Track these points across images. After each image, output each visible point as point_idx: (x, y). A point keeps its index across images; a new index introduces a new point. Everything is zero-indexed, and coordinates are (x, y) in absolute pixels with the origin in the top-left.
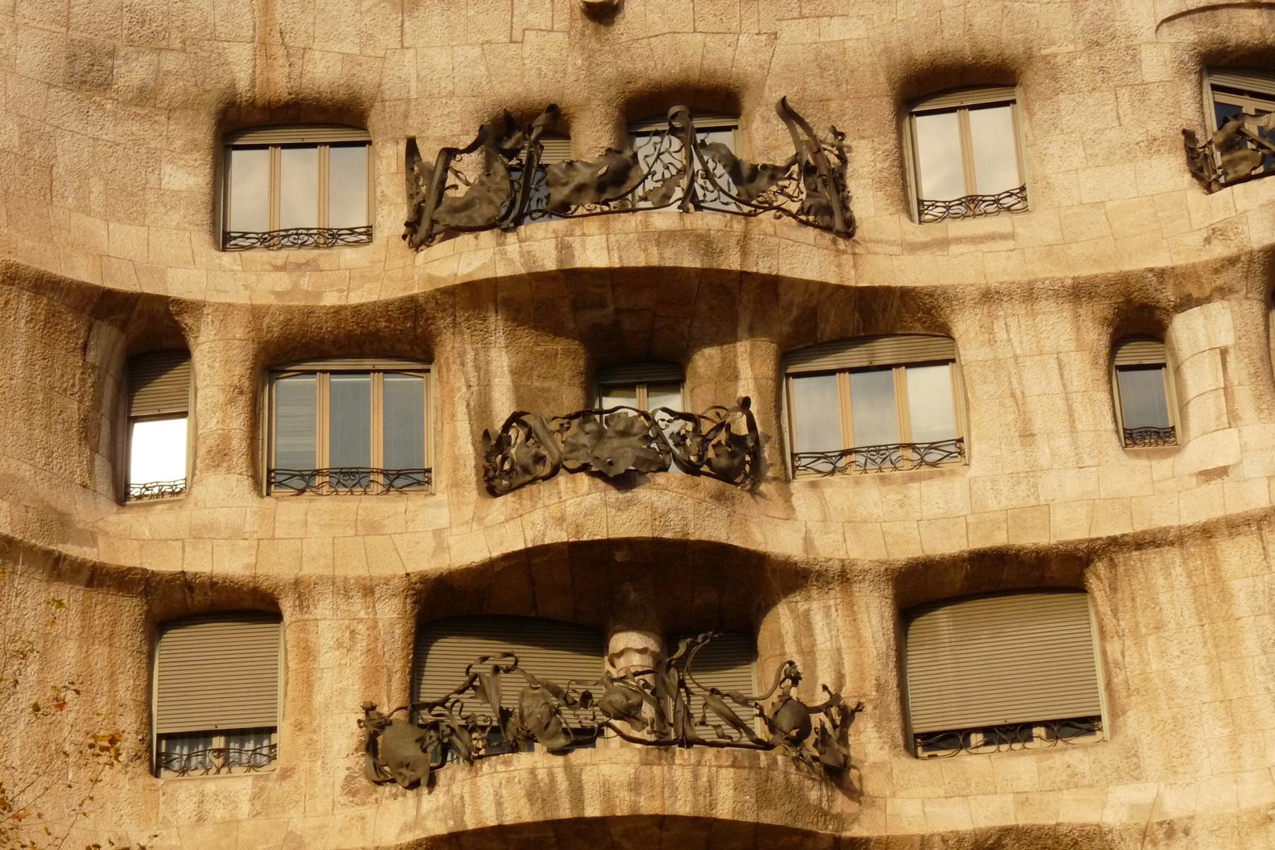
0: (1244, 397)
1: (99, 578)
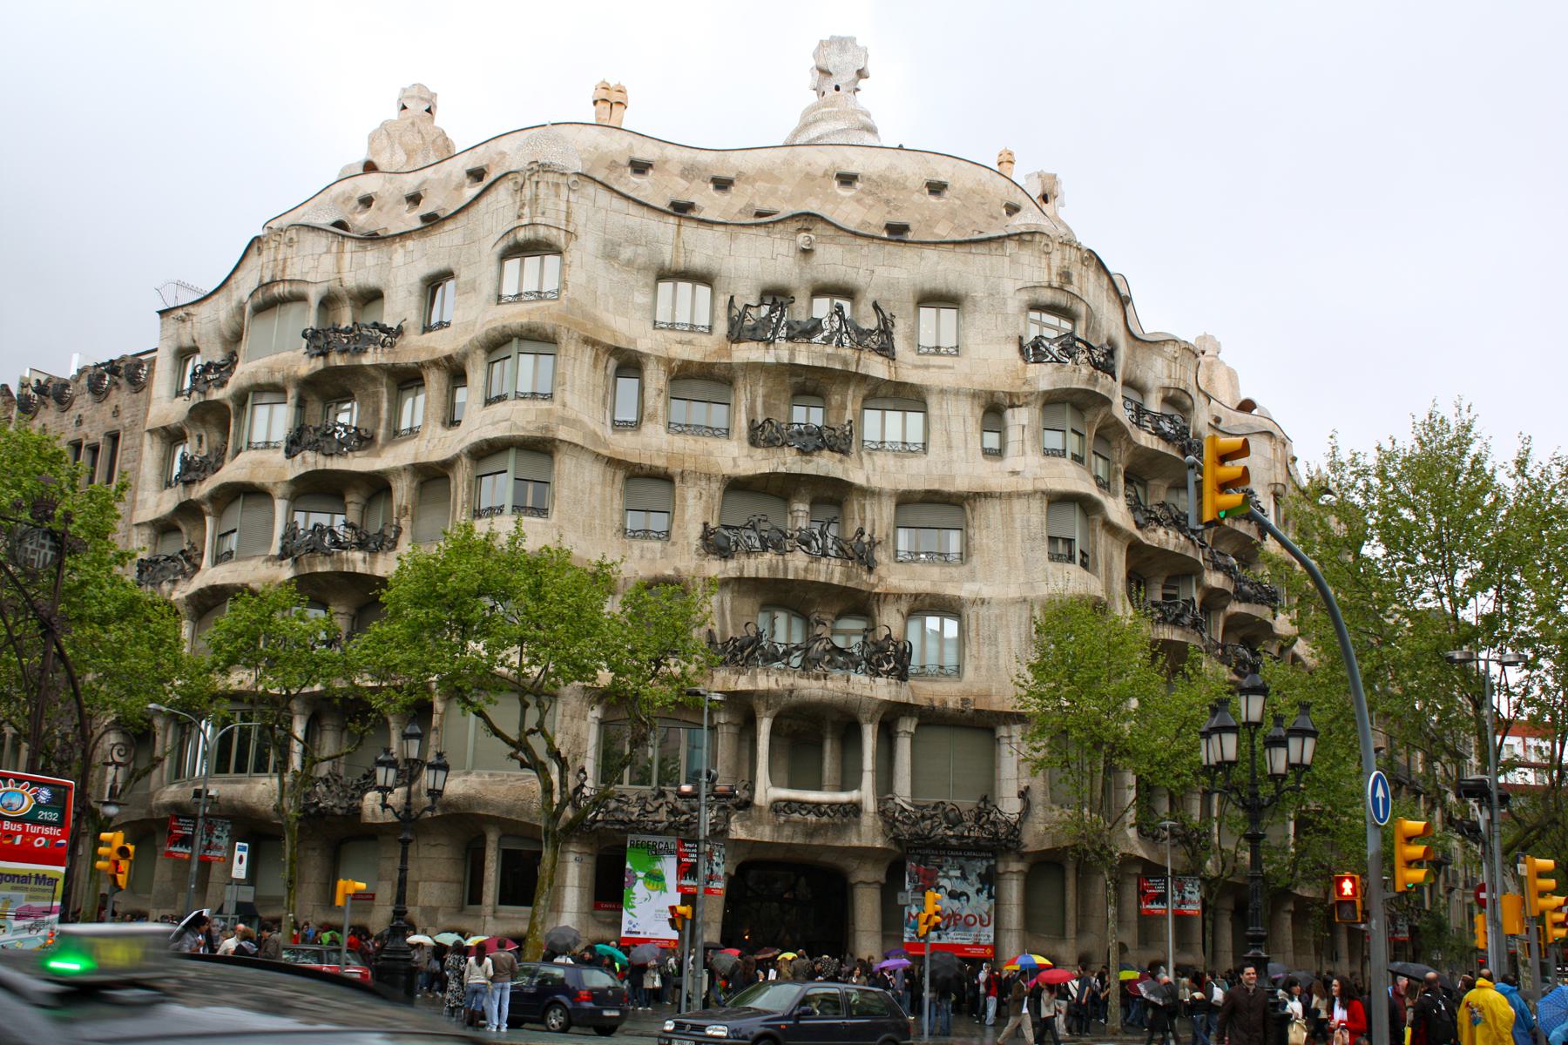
0: (1028, 445)
1: (613, 462)
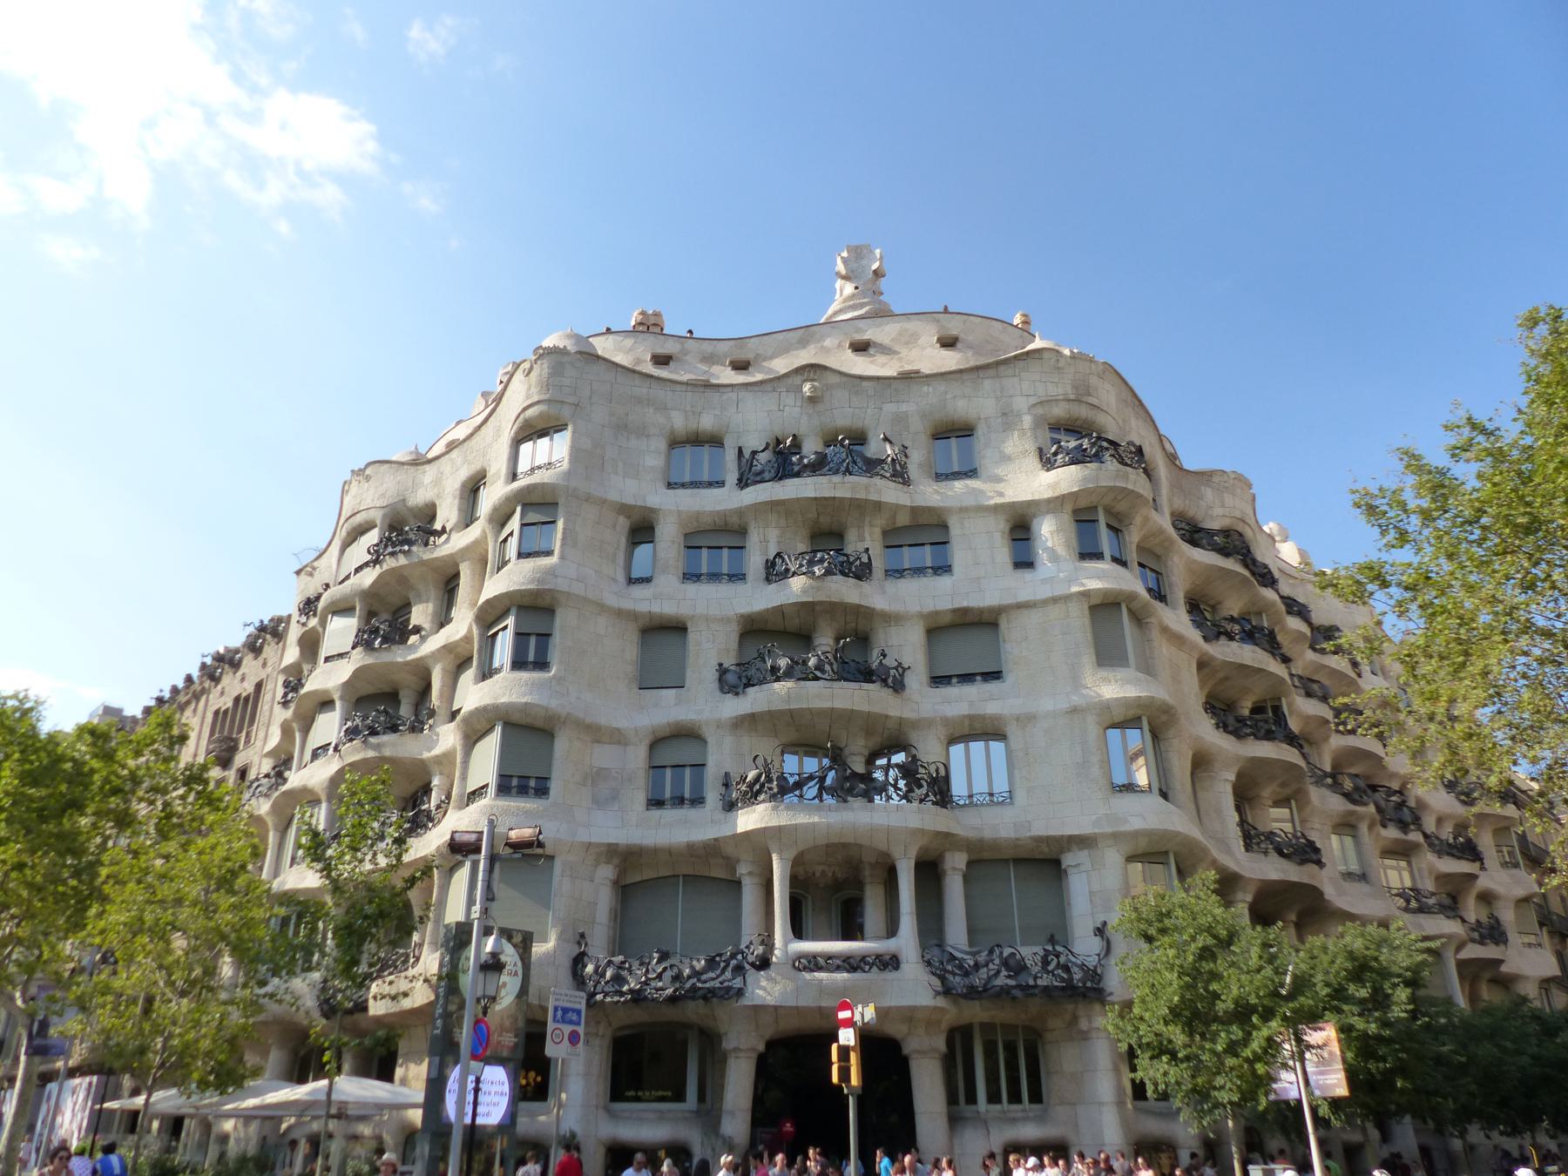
1: (620, 614)
